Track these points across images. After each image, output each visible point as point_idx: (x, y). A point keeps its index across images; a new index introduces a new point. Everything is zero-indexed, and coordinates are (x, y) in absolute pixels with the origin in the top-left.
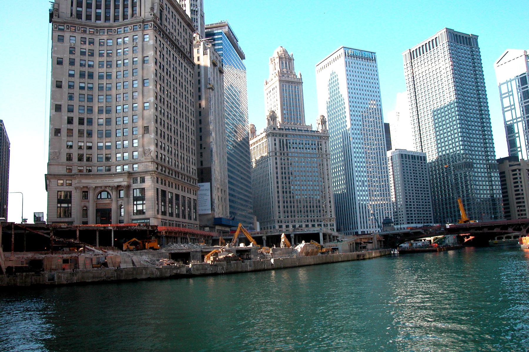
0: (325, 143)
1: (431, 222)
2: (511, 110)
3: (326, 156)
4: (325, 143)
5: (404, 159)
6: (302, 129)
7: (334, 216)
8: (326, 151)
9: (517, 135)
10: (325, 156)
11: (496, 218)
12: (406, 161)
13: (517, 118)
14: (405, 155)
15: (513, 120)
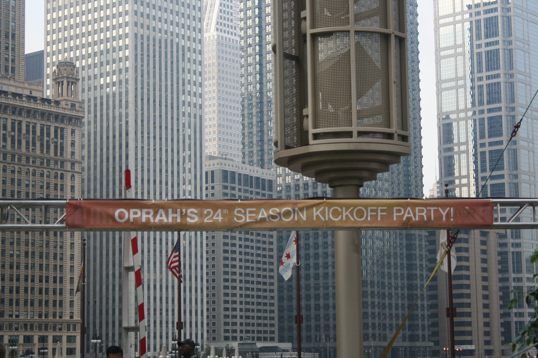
0: (73, 132)
1: (272, 339)
2: (457, 88)
3: (73, 164)
4: (73, 132)
5: (229, 184)
6: (19, 91)
7: (77, 317)
8: (73, 153)
9: (463, 148)
10: (68, 166)
11: (413, 338)
12: (233, 189)
13: (466, 110)
14: (233, 173)
15: (458, 111)
